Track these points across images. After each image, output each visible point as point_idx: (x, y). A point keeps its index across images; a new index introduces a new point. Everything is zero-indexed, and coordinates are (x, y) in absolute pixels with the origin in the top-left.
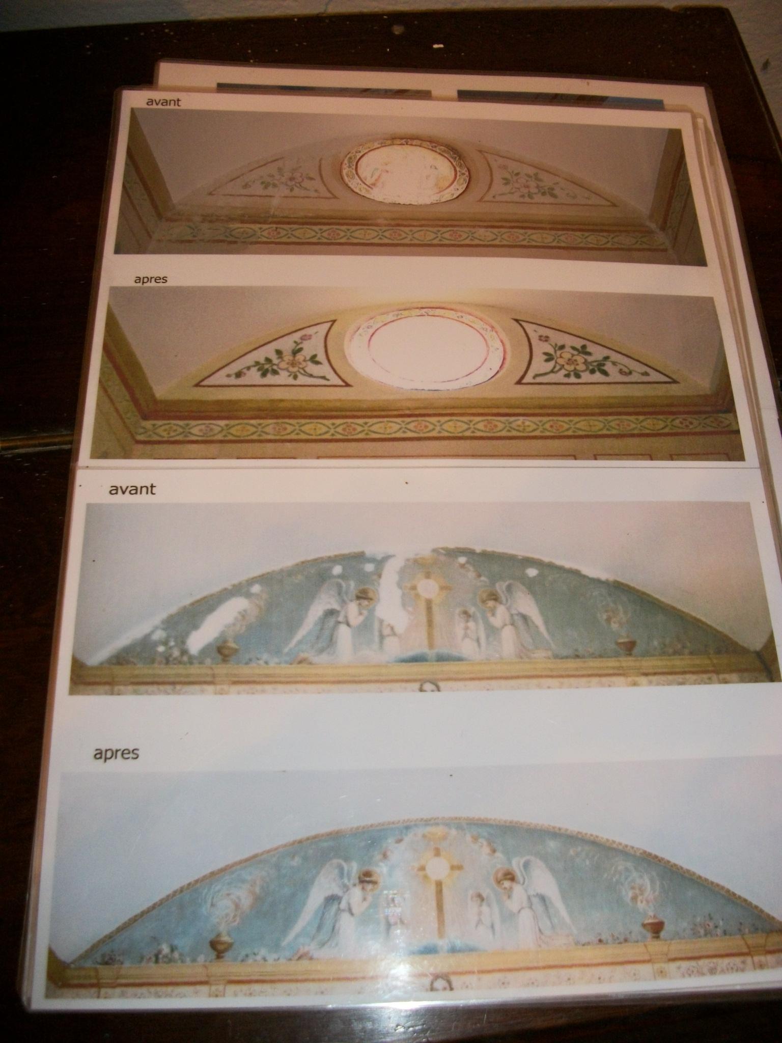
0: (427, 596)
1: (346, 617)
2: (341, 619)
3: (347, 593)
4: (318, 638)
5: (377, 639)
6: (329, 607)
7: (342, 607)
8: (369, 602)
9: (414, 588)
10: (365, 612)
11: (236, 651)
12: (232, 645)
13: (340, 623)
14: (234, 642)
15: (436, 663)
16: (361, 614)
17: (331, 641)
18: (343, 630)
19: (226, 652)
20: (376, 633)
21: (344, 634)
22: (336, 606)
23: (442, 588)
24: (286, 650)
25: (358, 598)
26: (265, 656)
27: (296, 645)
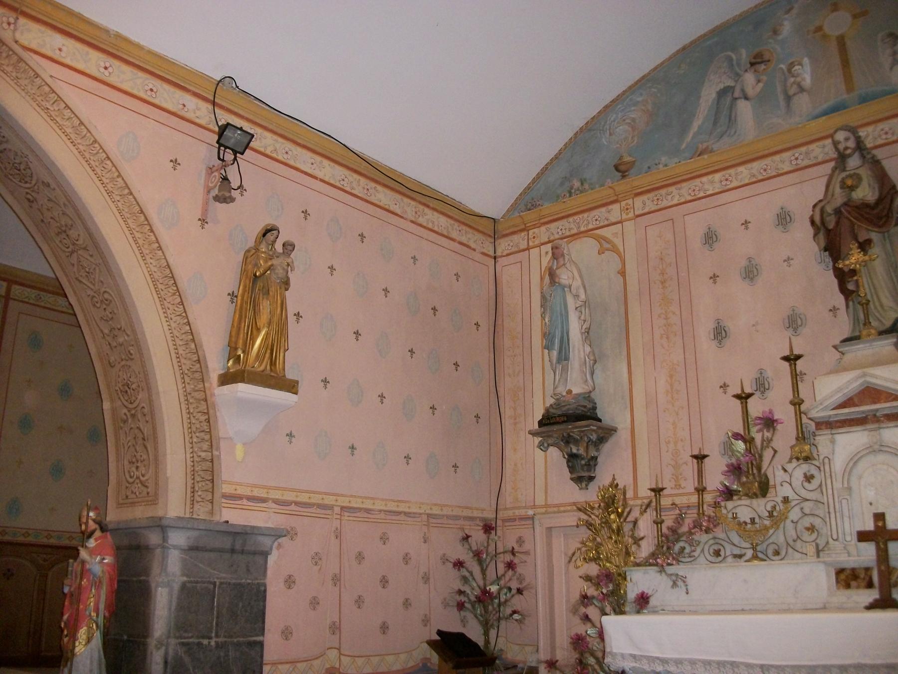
0: (837, 33)
1: (743, 90)
2: (737, 94)
3: (739, 65)
4: (715, 123)
5: (782, 103)
6: (722, 86)
7: (736, 81)
8: (765, 65)
9: (819, 29)
10: (764, 78)
11: (633, 163)
12: (627, 159)
13: (736, 99)
14: (630, 156)
15: (859, 106)
16: (759, 81)
17: (732, 120)
18: (743, 105)
19: (622, 168)
20: (781, 97)
21: (744, 109)
22: (730, 83)
23: (855, 17)
24: (684, 146)
25: (752, 64)
26: (664, 159)
27: (693, 138)
